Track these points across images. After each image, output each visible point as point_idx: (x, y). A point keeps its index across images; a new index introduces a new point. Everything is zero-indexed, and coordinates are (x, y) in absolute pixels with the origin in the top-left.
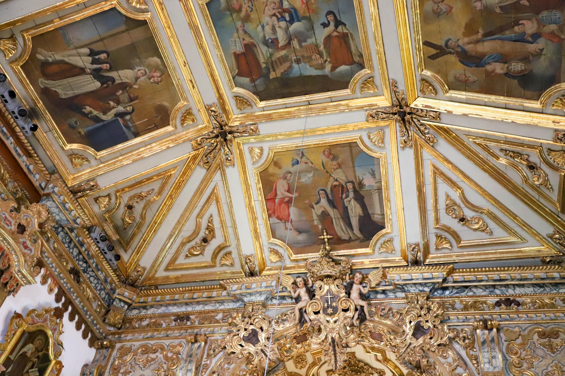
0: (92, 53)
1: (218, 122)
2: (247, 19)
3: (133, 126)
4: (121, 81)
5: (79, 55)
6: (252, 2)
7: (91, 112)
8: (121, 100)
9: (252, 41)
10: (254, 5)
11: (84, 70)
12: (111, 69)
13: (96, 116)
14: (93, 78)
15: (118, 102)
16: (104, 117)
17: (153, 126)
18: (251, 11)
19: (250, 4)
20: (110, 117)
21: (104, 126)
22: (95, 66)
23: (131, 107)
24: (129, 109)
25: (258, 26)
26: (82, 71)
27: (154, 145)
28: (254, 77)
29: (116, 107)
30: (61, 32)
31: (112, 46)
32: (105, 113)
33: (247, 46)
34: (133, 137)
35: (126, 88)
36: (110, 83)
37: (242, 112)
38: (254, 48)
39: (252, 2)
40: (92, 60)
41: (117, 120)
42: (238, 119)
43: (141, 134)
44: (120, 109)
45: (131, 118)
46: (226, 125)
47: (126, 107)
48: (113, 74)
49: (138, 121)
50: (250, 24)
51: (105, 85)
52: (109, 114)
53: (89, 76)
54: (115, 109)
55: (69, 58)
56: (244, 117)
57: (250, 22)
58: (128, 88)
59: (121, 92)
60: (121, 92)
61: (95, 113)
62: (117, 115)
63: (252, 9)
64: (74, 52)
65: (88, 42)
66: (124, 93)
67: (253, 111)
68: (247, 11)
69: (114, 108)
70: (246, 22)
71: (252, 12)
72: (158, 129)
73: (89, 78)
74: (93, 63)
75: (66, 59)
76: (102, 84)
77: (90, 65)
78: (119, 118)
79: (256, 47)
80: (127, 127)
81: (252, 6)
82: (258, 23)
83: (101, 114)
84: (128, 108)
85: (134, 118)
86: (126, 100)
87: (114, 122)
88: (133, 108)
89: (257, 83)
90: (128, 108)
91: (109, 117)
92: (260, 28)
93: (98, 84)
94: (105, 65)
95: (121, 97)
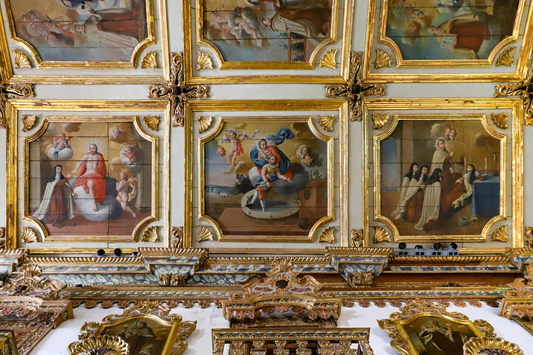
0: (410, 176)
1: (516, 90)
2: (428, 21)
3: (487, 173)
4: (442, 164)
5: (407, 186)
6: (415, 10)
7: (460, 202)
8: (458, 172)
9: (449, 23)
10: (418, 9)
11: (421, 189)
12: (429, 168)
13: (465, 200)
14: (430, 186)
15: (460, 175)
16: (469, 194)
17: (495, 155)
18: (423, 14)
19: (417, 12)
20: (471, 188)
21: (476, 198)
22: (421, 179)
23: (469, 166)
24: (469, 169)
25: (437, 11)
26: (421, 191)
27: (514, 162)
28: (484, 34)
29: (463, 179)
30: (384, 191)
31: (410, 155)
32: (465, 191)
33: (453, 31)
34: (497, 177)
35: (449, 163)
36: (440, 174)
37: (515, 62)
38: (457, 22)
39: (415, 10)
40: (415, 178)
41: (475, 183)
42: (522, 68)
43: (498, 169)
44: (466, 176)
45: (479, 171)
46: (523, 82)
47: (467, 170)
48: (434, 167)
49: (484, 167)
50: (433, 19)
51: (440, 179)
52: (467, 188)
53: (427, 188)
54: (465, 180)
55: (406, 196)
56: (522, 60)
57: (432, 18)
58: (450, 161)
59: (451, 169)
60: (451, 169)
61: (461, 199)
62: (471, 182)
63: (421, 12)
64: (403, 189)
65: (400, 177)
66: (454, 167)
67: (518, 49)
68: (421, 18)
69: (463, 181)
70: (430, 22)
71: (424, 13)
72: (499, 152)
73: (428, 189)
74: (417, 179)
75: (407, 198)
76: (438, 181)
77: (418, 182)
78: (475, 182)
79: (456, 20)
80: (486, 178)
81: (418, 10)
82: (435, 10)
83: (464, 194)
84: (469, 170)
85: (480, 169)
86: (461, 167)
87: (477, 187)
88: (470, 165)
89: (491, 33)
90: (469, 170)
91: (470, 190)
92: (440, 10)
93: (437, 184)
94: (423, 171)
95: (455, 172)
